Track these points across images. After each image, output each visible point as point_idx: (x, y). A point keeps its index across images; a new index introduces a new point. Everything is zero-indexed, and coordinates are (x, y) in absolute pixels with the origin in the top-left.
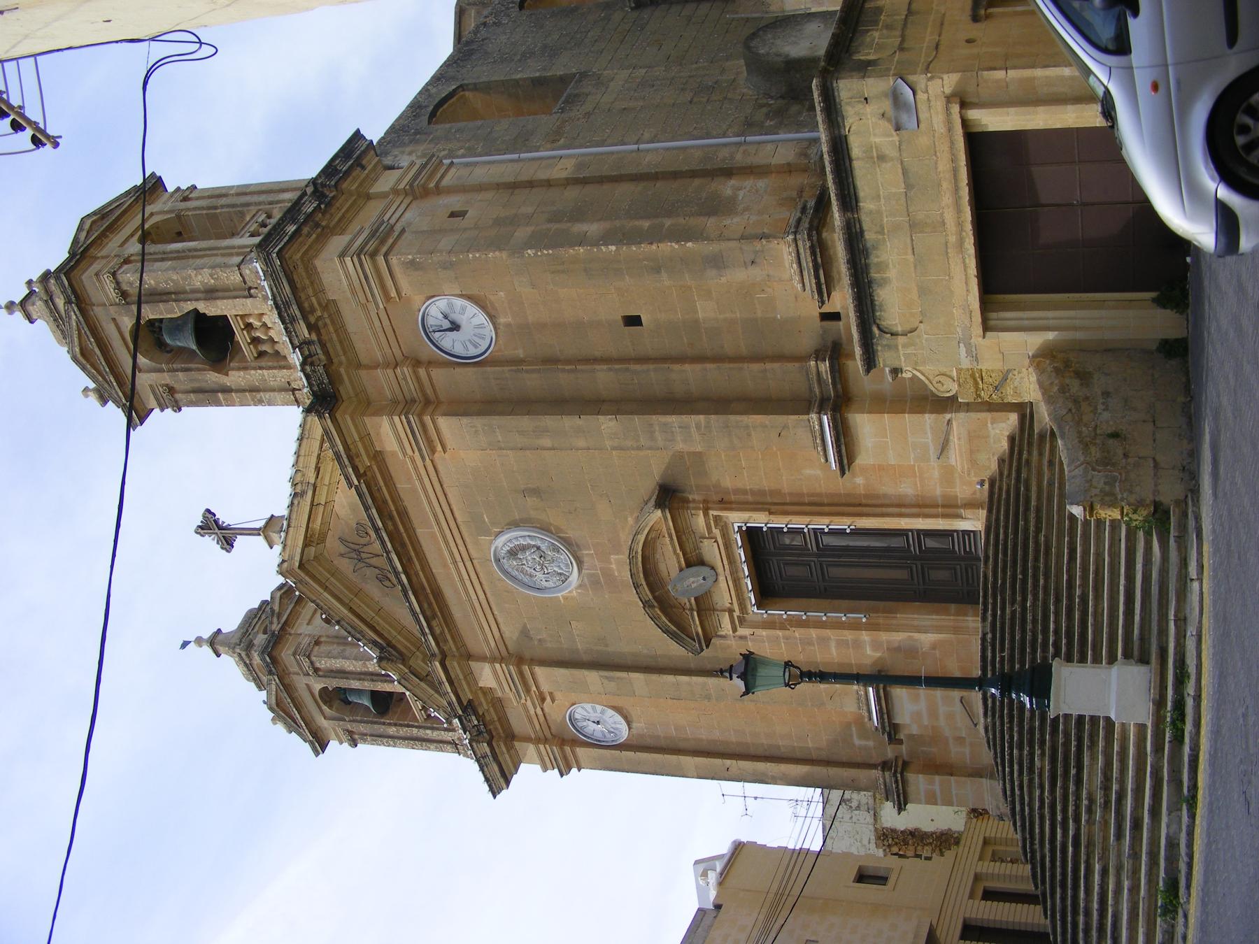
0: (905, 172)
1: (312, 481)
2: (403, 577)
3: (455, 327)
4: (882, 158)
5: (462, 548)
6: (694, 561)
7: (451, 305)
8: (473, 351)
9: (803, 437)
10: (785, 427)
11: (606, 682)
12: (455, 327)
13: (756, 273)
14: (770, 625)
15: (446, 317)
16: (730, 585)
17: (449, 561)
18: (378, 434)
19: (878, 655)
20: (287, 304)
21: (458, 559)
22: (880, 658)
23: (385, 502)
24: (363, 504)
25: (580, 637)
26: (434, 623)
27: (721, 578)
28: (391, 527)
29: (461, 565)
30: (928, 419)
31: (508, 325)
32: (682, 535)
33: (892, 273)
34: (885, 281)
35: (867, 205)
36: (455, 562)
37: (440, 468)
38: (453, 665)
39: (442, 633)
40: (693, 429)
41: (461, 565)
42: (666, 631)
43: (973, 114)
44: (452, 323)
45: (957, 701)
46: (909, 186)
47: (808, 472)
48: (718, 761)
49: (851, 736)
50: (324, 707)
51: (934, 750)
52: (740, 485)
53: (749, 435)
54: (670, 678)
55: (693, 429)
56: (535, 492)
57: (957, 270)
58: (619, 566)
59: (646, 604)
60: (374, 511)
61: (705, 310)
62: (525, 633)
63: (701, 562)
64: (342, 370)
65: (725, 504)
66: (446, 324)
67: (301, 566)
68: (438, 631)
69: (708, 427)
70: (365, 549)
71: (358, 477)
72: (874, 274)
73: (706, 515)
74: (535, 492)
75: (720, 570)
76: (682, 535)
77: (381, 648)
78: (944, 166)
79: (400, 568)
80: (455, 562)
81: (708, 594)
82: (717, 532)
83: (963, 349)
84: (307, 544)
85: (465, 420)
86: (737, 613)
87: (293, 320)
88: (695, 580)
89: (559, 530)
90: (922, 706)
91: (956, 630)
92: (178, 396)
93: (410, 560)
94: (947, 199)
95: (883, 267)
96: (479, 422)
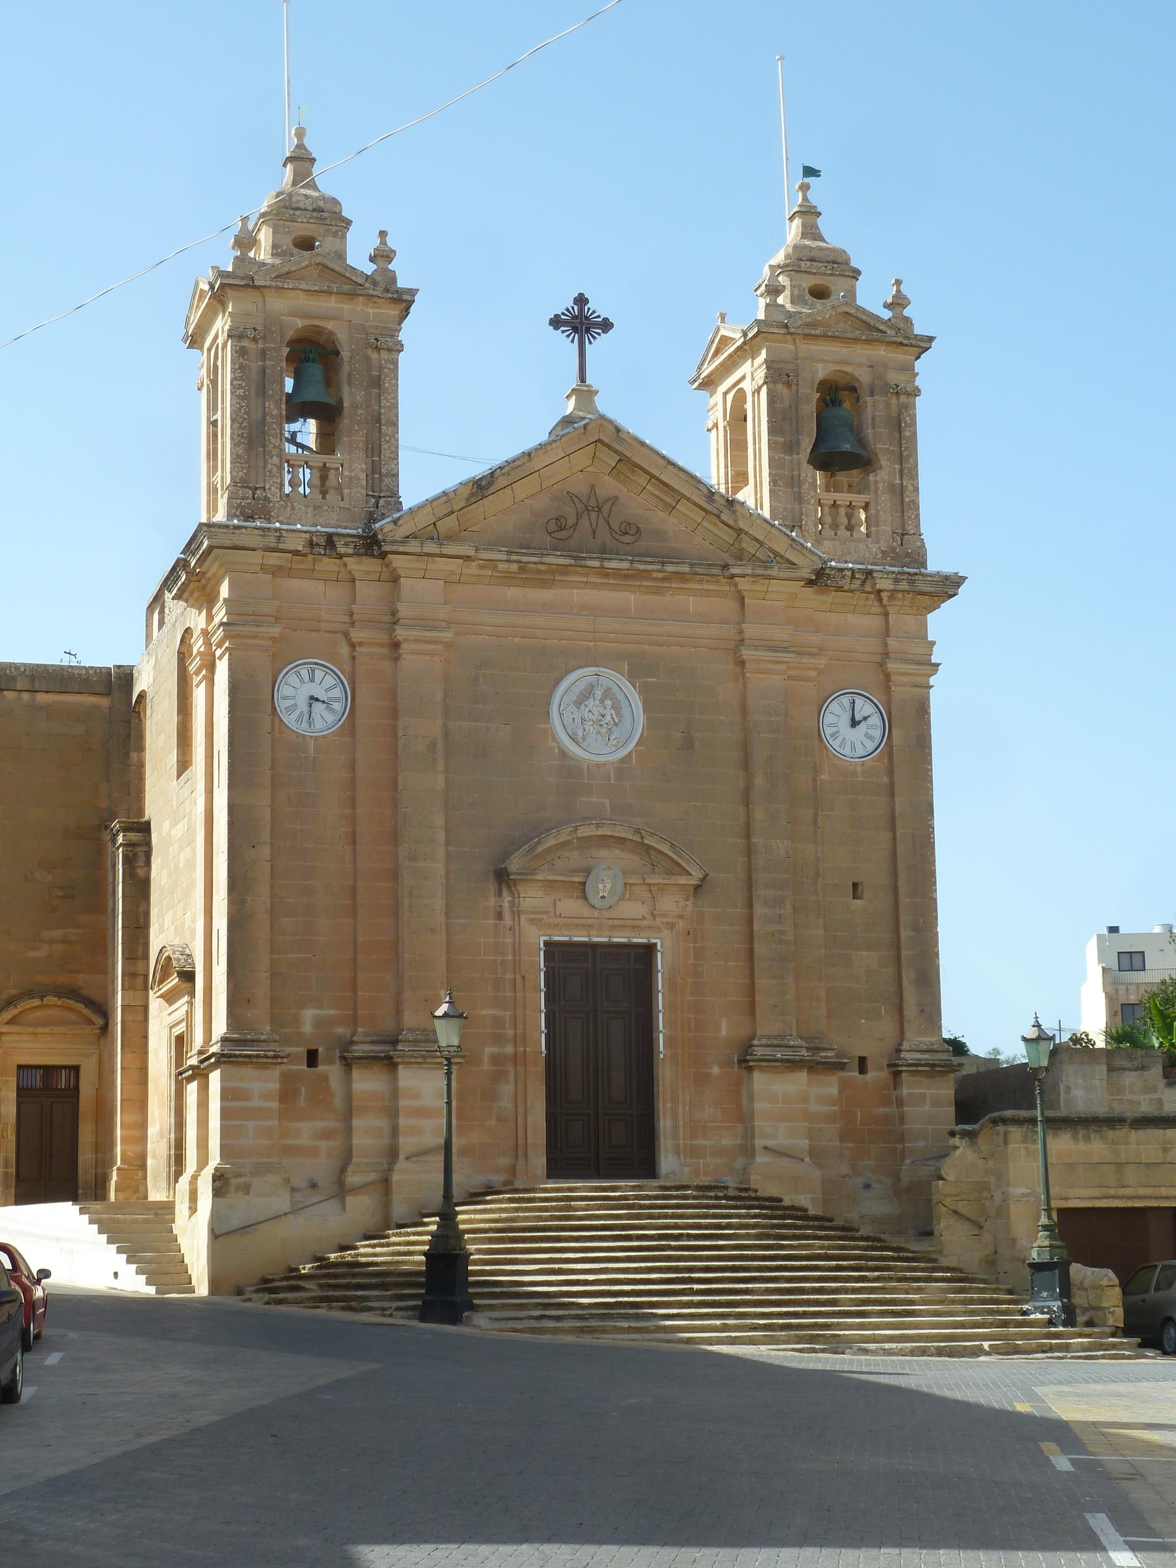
1: (723, 517)
3: (854, 723)
4: (1165, 1150)
8: (828, 731)
12: (854, 723)
15: (865, 719)
28: (655, 575)
33: (1082, 1146)
35: (1135, 1135)
40: (777, 927)
44: (859, 722)
46: (1148, 1165)
47: (724, 1023)
51: (302, 1103)
53: (774, 978)
55: (777, 927)
57: (1096, 1192)
66: (858, 717)
70: (601, 521)
72: (1081, 1132)
93: (607, 575)
95: (1087, 1139)
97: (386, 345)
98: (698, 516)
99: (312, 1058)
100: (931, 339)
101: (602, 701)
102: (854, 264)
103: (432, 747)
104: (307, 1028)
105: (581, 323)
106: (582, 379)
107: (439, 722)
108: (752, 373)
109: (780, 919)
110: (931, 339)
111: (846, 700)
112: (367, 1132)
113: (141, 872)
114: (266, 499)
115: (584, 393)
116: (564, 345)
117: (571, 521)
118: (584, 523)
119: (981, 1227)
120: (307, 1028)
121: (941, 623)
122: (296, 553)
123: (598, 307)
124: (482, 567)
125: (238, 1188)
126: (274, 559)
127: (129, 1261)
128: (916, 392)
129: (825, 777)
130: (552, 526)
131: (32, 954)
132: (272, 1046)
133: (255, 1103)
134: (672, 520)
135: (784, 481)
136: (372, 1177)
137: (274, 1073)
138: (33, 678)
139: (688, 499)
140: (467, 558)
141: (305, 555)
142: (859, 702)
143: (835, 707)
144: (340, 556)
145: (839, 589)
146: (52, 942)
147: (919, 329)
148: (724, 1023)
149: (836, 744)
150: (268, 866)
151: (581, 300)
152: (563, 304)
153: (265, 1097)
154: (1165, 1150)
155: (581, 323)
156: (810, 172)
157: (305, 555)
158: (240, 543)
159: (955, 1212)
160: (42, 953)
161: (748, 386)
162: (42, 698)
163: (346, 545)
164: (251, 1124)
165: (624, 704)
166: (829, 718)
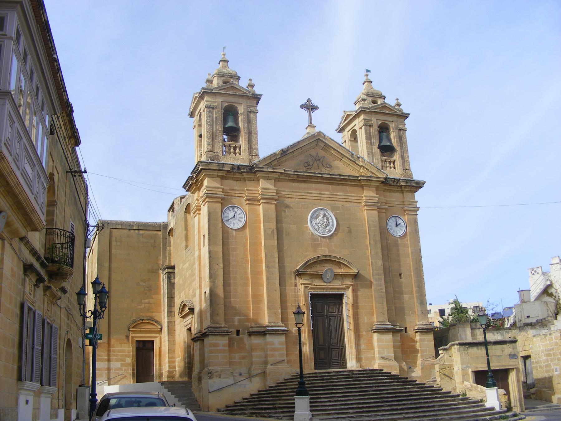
0: (501, 356)
2: (320, 175)
3: (397, 226)
4: (503, 351)
5: (325, 199)
6: (336, 276)
7: (402, 226)
8: (389, 228)
9: (382, 319)
10: (384, 314)
11: (271, 230)
12: (397, 226)
13: (420, 313)
14: (305, 295)
16: (321, 286)
17: (322, 192)
18: (370, 190)
19: (294, 332)
20: (411, 183)
21: (321, 196)
22: (292, 332)
23: (346, 181)
24: (351, 176)
25: (289, 227)
26: (296, 176)
27: (326, 284)
29: (319, 195)
30: (393, 355)
31: (398, 241)
32: (343, 276)
33: (480, 351)
34: (478, 349)
36: (320, 194)
37: (356, 204)
38: (276, 176)
39: (290, 177)
40: (380, 287)
41: (319, 195)
42: (308, 261)
43: (515, 370)
45: (283, 359)
46: (498, 356)
47: (366, 318)
48: (221, 261)
49: (240, 316)
50: (227, 104)
51: (236, 348)
52: (359, 297)
54: (276, 255)
55: (380, 287)
56: (350, 231)
58: (323, 251)
59: (319, 257)
60: (347, 178)
61: (406, 297)
62: (287, 206)
63: (333, 279)
64: (386, 187)
65: (353, 290)
67: (319, 139)
68: (291, 176)
69: (382, 292)
71: (361, 179)
72: (479, 347)
73: (351, 285)
74: (350, 231)
75: (329, 284)
76: (343, 276)
77: (285, 152)
78: (504, 364)
79: (324, 176)
80: (320, 194)
81: (322, 278)
82: (344, 286)
83: (465, 366)
84: (326, 145)
85: (377, 220)
86: (310, 286)
87: (407, 182)
88: (329, 276)
89: (336, 235)
90: (277, 346)
91: (310, 359)
92: (368, 127)
93: (323, 179)
94: (497, 364)
96: (377, 223)
97: (252, 113)
98: (348, 162)
99: (238, 332)
100: (409, 114)
101: (323, 218)
102: (383, 95)
103: (273, 231)
104: (236, 323)
105: (310, 107)
106: (311, 123)
107: (275, 224)
108: (358, 123)
109: (381, 285)
110: (409, 114)
111: (394, 219)
112: (257, 356)
113: (172, 281)
114: (218, 155)
115: (312, 126)
116: (305, 113)
117: (311, 163)
118: (315, 164)
119: (451, 378)
120: (236, 323)
121: (419, 195)
122: (228, 171)
123: (314, 102)
124: (286, 176)
125: (216, 376)
126: (221, 174)
127: (179, 401)
128: (405, 130)
129: (390, 241)
130: (306, 165)
131: (139, 307)
132: (226, 329)
133: (221, 348)
134: (341, 163)
135: (371, 153)
136: (260, 371)
137: (226, 338)
138: (139, 226)
139: (346, 157)
140: (281, 173)
141: (231, 172)
142: (398, 219)
143: (391, 221)
144: (242, 172)
145: (390, 185)
146: (145, 303)
147: (405, 111)
148: (366, 318)
149: (392, 232)
150: (222, 270)
151: (309, 100)
152: (304, 101)
153: (223, 346)
154: (503, 351)
155: (310, 107)
156: (368, 71)
157: (231, 172)
158: (211, 168)
159: (444, 374)
160: (142, 307)
161: (356, 128)
162: (141, 232)
163: (244, 169)
164: (220, 354)
165: (330, 218)
166: (389, 224)
